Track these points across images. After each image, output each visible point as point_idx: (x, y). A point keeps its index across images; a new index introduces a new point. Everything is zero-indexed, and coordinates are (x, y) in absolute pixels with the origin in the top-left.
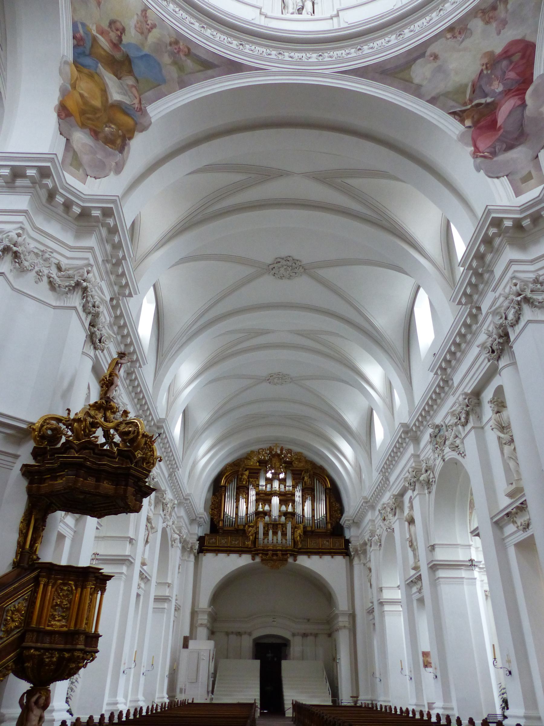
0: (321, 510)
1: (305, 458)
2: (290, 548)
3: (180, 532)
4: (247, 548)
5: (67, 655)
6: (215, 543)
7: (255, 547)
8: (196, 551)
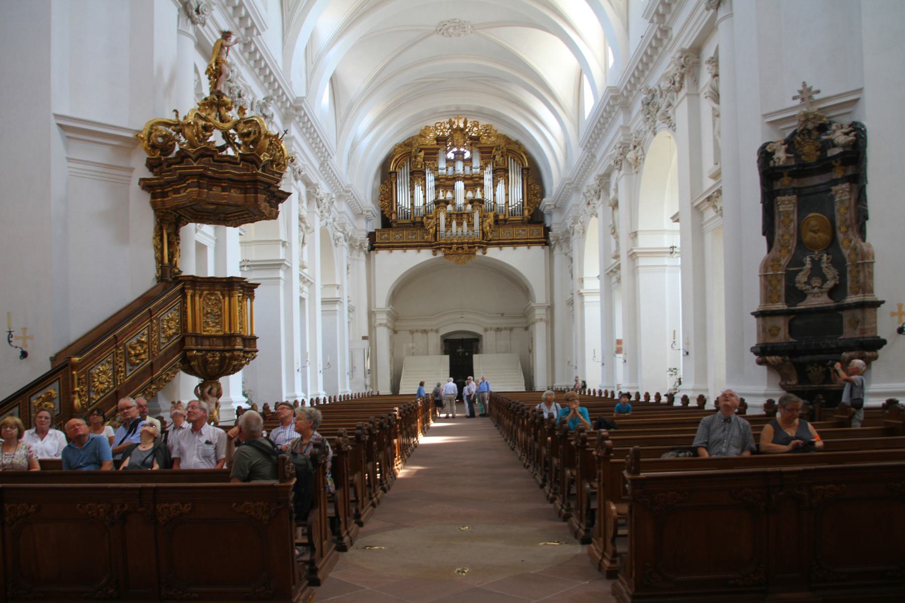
0: (517, 195)
1: (496, 131)
2: (478, 240)
3: (344, 229)
4: (426, 242)
5: (228, 355)
6: (388, 239)
7: (436, 240)
8: (366, 249)
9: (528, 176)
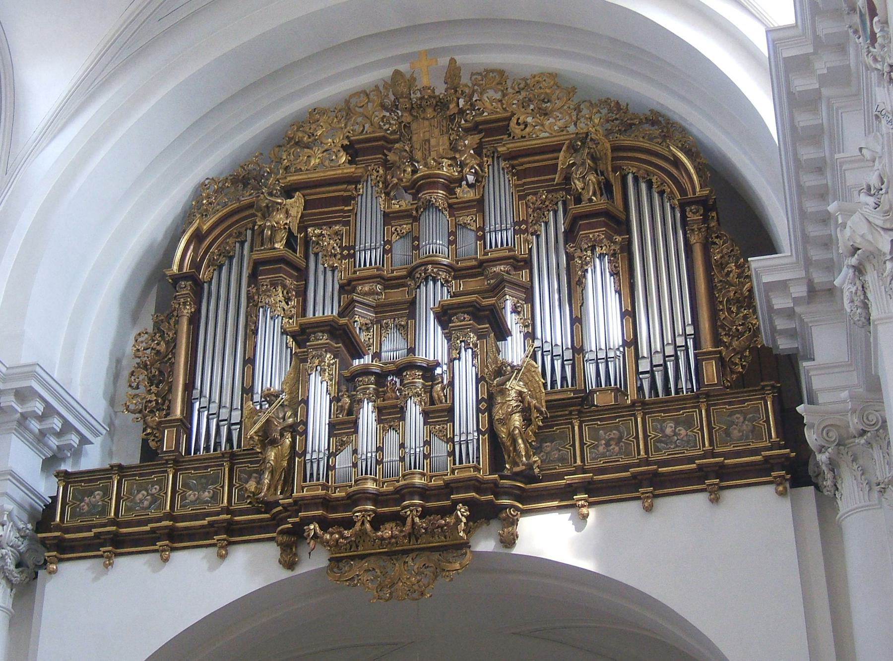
1: (571, 91)
9: (708, 228)
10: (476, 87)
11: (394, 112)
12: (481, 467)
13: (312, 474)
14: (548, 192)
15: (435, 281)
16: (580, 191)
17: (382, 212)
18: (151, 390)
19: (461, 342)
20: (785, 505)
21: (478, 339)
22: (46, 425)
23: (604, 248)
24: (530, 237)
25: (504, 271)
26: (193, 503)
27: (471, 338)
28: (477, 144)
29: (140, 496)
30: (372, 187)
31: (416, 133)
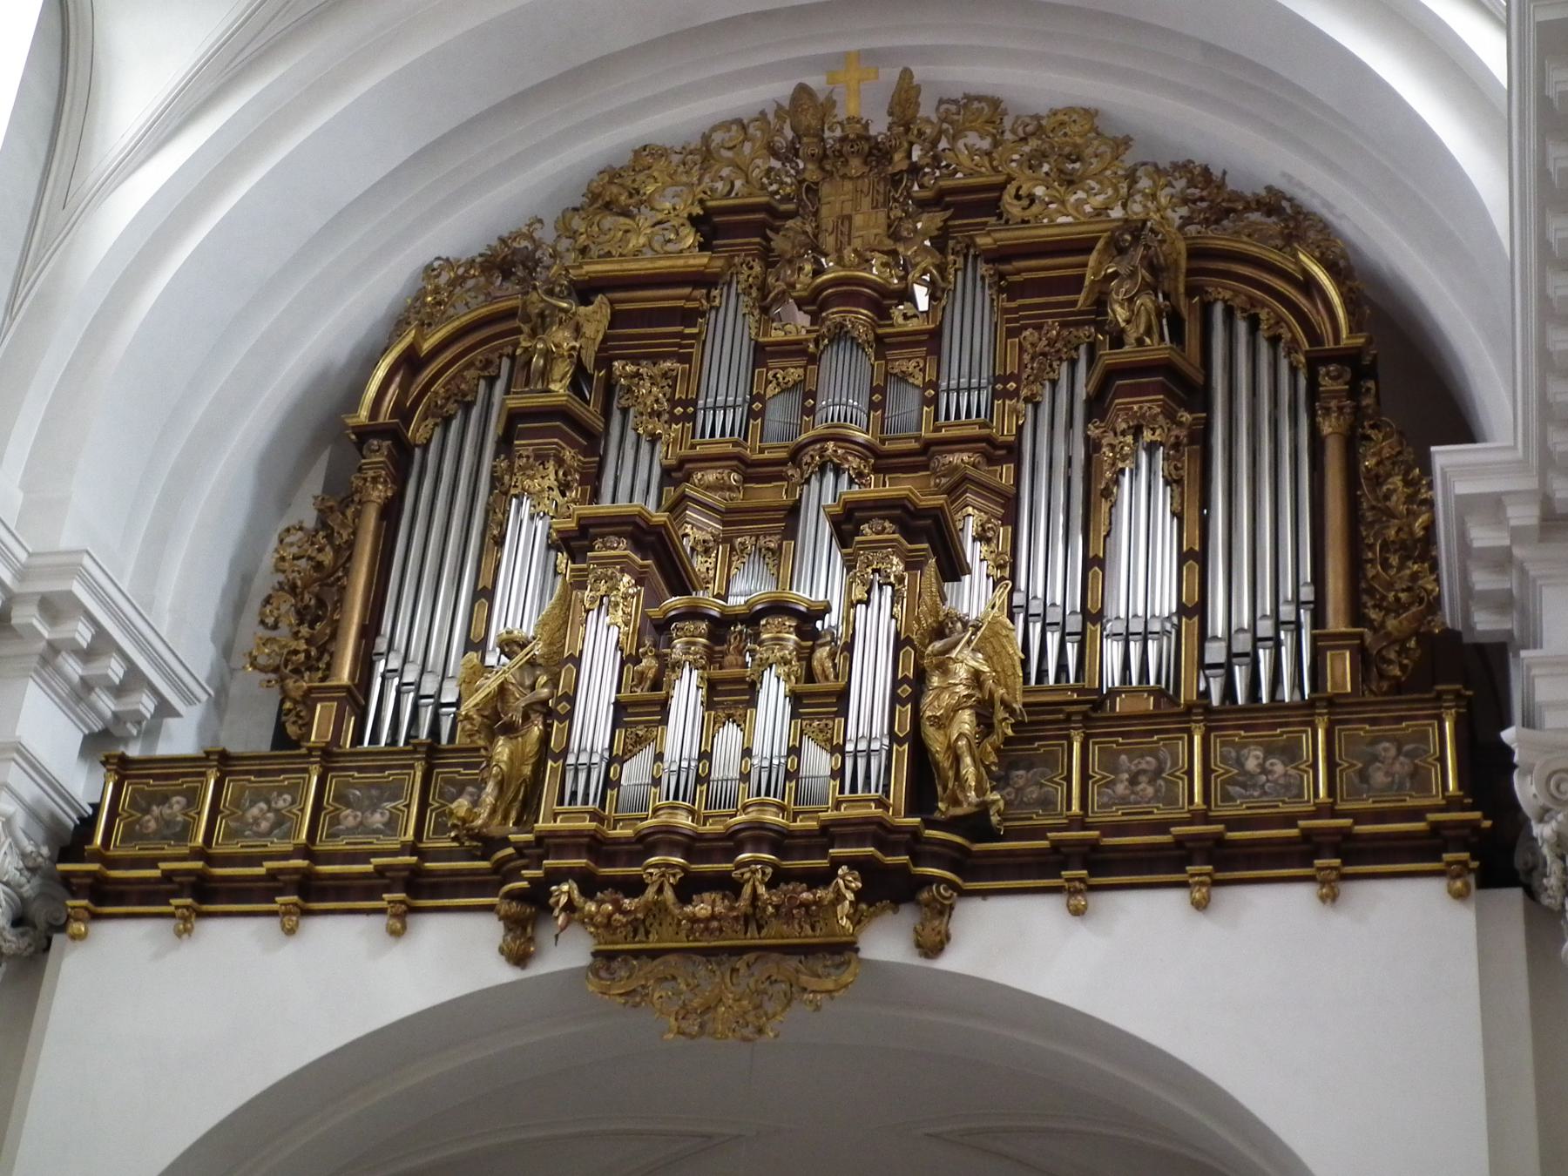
1: (1123, 143)
9: (1358, 410)
10: (945, 126)
11: (791, 161)
12: (891, 801)
13: (574, 794)
14: (1063, 325)
15: (838, 471)
16: (1123, 324)
17: (753, 342)
18: (299, 632)
19: (874, 571)
20: (1463, 919)
21: (906, 569)
22: (95, 669)
23: (1158, 432)
24: (1021, 405)
25: (968, 463)
26: (350, 831)
27: (892, 565)
28: (938, 229)
29: (255, 811)
30: (738, 295)
31: (829, 203)
